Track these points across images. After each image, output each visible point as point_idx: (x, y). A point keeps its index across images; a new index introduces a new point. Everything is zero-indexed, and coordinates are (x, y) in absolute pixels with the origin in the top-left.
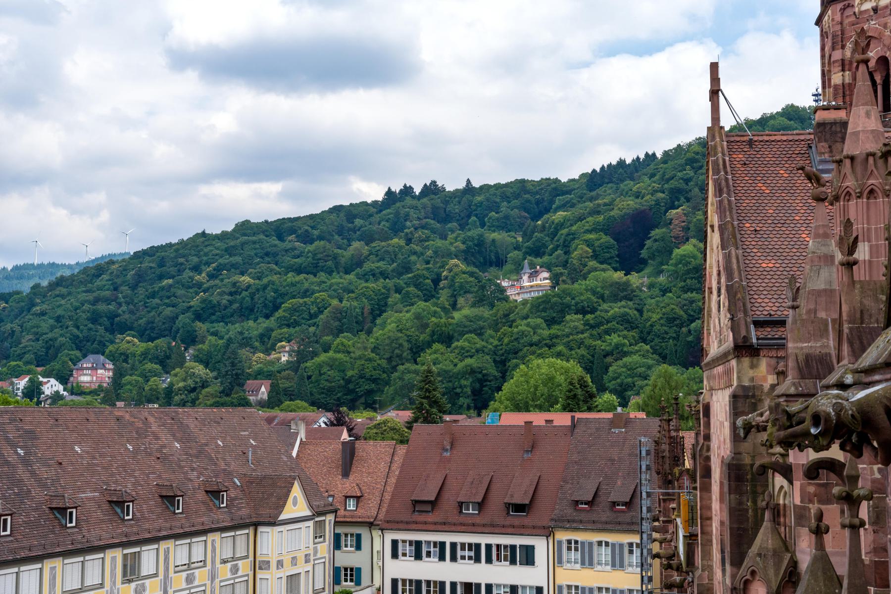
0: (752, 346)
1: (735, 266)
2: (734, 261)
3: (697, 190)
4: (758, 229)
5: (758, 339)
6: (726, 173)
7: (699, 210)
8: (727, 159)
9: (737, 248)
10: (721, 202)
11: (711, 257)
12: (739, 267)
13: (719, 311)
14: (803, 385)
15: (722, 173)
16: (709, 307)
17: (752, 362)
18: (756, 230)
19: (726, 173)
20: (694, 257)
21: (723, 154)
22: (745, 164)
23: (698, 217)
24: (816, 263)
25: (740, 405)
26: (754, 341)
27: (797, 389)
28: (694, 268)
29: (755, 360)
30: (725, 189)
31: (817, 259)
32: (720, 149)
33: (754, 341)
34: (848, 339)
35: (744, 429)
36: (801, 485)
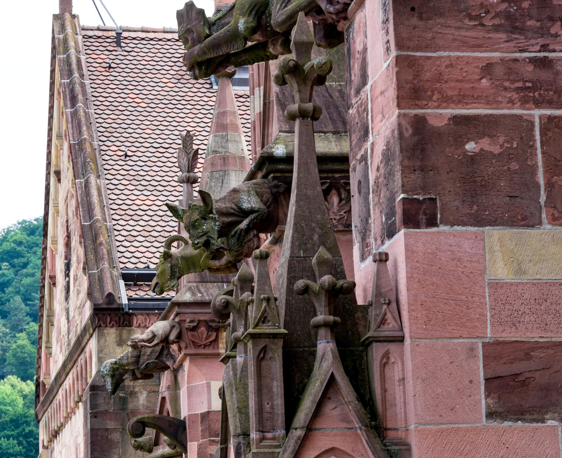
0: (120, 308)
1: (95, 199)
2: (94, 192)
3: (18, 298)
4: (129, 153)
5: (129, 300)
6: (82, 76)
7: (21, 331)
8: (83, 58)
9: (98, 177)
10: (75, 114)
11: (55, 226)
12: (101, 201)
13: (67, 298)
14: (203, 290)
15: (76, 75)
16: (51, 309)
17: (120, 335)
18: (126, 156)
19: (82, 76)
20: (12, 403)
21: (78, 52)
22: (110, 67)
23: (20, 342)
24: (219, 168)
25: (101, 401)
26: (125, 301)
27: (194, 294)
28: (12, 421)
29: (125, 332)
30: (80, 97)
31: (219, 162)
32: (72, 44)
33: (125, 301)
34: (279, 100)
35: (113, 376)
36: (200, 447)
